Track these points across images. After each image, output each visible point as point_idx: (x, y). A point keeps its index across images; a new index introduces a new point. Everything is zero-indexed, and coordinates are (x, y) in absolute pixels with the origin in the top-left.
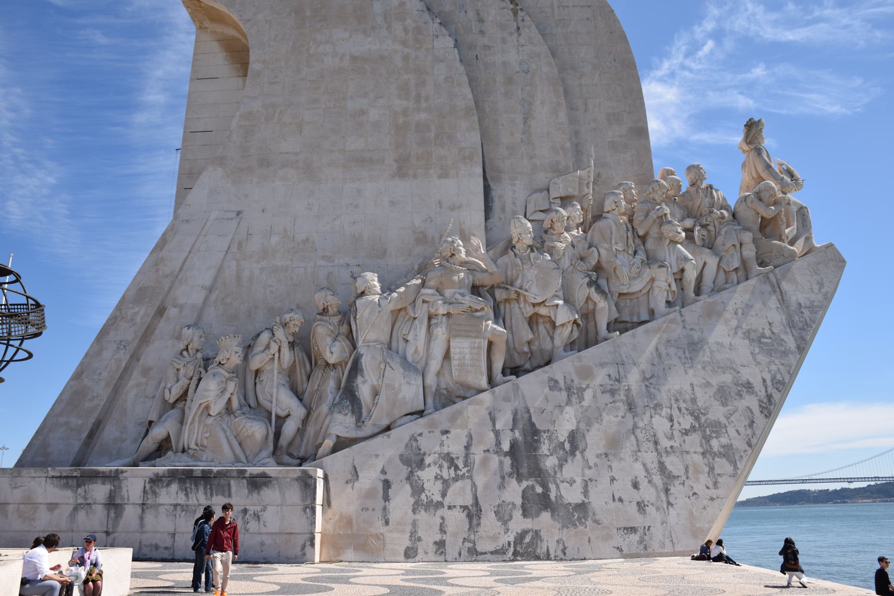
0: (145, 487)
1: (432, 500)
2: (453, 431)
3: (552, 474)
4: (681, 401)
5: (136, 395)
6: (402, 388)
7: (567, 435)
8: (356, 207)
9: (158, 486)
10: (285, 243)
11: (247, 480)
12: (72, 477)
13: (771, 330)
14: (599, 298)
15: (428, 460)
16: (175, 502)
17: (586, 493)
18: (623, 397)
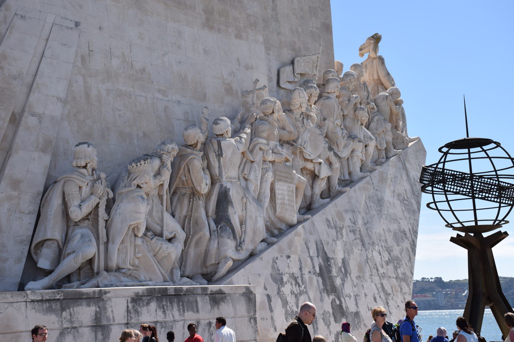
0: (128, 307)
1: (293, 310)
2: (292, 256)
3: (341, 290)
4: (382, 241)
5: (9, 210)
6: (258, 220)
7: (341, 262)
8: (179, 47)
9: (140, 306)
10: (125, 69)
11: (209, 296)
12: (54, 300)
13: (407, 195)
14: (336, 160)
15: (285, 279)
16: (155, 320)
17: (357, 304)
18: (359, 236)
